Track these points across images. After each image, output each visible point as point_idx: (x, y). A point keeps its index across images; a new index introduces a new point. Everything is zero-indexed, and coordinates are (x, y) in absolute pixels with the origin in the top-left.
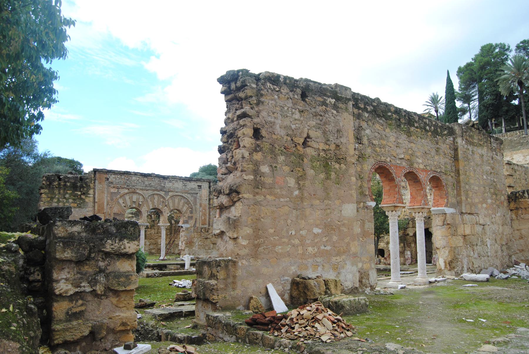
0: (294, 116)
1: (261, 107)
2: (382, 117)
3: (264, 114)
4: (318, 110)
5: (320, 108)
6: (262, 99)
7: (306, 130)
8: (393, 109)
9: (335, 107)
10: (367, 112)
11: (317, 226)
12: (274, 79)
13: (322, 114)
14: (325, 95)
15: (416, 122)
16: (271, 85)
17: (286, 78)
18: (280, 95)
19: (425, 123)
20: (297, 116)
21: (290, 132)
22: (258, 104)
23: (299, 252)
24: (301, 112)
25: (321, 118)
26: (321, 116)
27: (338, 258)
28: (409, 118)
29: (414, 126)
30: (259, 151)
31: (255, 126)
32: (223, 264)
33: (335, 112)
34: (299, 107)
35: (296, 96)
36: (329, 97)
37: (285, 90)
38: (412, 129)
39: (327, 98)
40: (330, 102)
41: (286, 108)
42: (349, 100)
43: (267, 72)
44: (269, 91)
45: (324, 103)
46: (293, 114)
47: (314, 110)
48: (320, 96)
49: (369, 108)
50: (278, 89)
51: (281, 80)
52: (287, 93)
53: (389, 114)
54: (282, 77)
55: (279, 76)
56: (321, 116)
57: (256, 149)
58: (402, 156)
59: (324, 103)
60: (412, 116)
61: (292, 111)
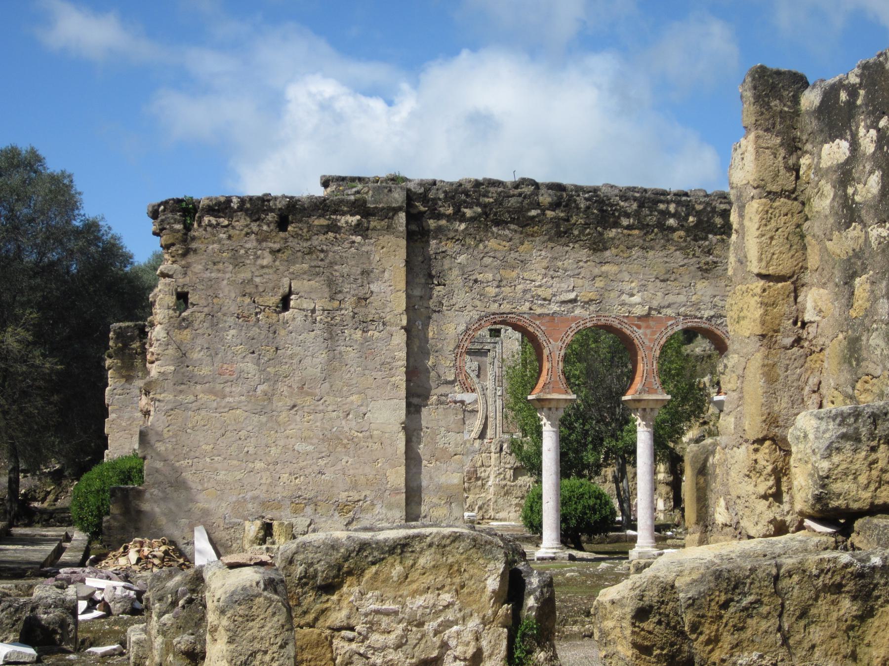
0: (259, 262)
1: (191, 258)
2: (507, 223)
3: (198, 268)
4: (315, 243)
5: (322, 237)
6: (194, 245)
7: (286, 281)
8: (545, 198)
9: (358, 229)
10: (463, 218)
11: (304, 439)
12: (221, 208)
13: (325, 248)
14: (335, 212)
15: (628, 215)
16: (211, 218)
17: (242, 201)
18: (231, 232)
19: (666, 214)
20: (267, 260)
21: (249, 289)
22: (184, 255)
23: (263, 481)
24: (274, 252)
25: (322, 255)
26: (322, 251)
27: (351, 494)
28: (601, 211)
29: (616, 224)
30: (186, 328)
31: (179, 290)
32: (119, 494)
33: (358, 239)
34: (271, 245)
35: (265, 228)
36: (344, 214)
37: (241, 222)
38: (612, 233)
39: (339, 217)
40: (347, 222)
41: (242, 252)
42: (396, 210)
43: (210, 199)
44: (209, 229)
45: (334, 228)
46: (257, 257)
47: (306, 244)
48: (322, 216)
49: (468, 213)
50: (226, 223)
51: (235, 205)
52: (247, 226)
53: (533, 213)
54: (235, 200)
55: (229, 200)
56: (322, 251)
57: (183, 324)
58: (572, 296)
59: (334, 228)
60: (612, 205)
61: (255, 254)
